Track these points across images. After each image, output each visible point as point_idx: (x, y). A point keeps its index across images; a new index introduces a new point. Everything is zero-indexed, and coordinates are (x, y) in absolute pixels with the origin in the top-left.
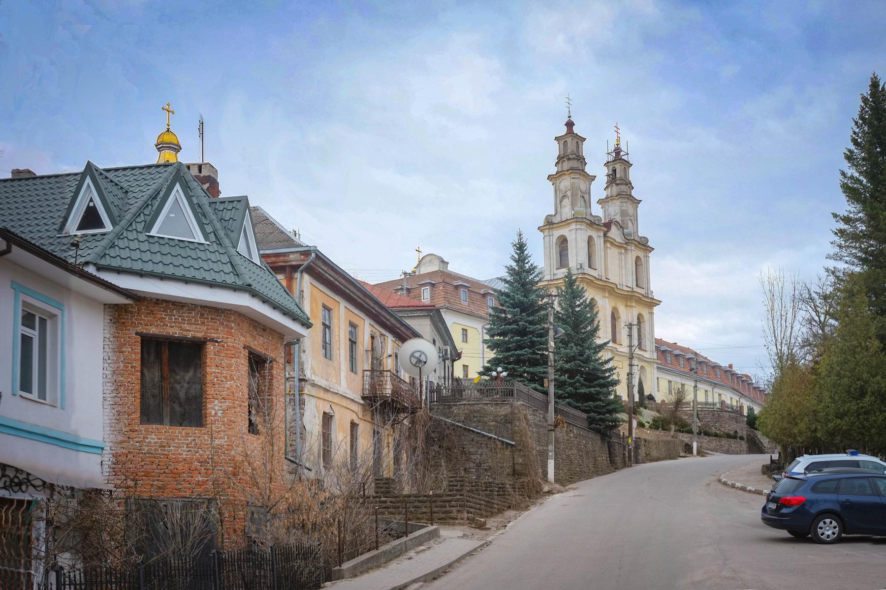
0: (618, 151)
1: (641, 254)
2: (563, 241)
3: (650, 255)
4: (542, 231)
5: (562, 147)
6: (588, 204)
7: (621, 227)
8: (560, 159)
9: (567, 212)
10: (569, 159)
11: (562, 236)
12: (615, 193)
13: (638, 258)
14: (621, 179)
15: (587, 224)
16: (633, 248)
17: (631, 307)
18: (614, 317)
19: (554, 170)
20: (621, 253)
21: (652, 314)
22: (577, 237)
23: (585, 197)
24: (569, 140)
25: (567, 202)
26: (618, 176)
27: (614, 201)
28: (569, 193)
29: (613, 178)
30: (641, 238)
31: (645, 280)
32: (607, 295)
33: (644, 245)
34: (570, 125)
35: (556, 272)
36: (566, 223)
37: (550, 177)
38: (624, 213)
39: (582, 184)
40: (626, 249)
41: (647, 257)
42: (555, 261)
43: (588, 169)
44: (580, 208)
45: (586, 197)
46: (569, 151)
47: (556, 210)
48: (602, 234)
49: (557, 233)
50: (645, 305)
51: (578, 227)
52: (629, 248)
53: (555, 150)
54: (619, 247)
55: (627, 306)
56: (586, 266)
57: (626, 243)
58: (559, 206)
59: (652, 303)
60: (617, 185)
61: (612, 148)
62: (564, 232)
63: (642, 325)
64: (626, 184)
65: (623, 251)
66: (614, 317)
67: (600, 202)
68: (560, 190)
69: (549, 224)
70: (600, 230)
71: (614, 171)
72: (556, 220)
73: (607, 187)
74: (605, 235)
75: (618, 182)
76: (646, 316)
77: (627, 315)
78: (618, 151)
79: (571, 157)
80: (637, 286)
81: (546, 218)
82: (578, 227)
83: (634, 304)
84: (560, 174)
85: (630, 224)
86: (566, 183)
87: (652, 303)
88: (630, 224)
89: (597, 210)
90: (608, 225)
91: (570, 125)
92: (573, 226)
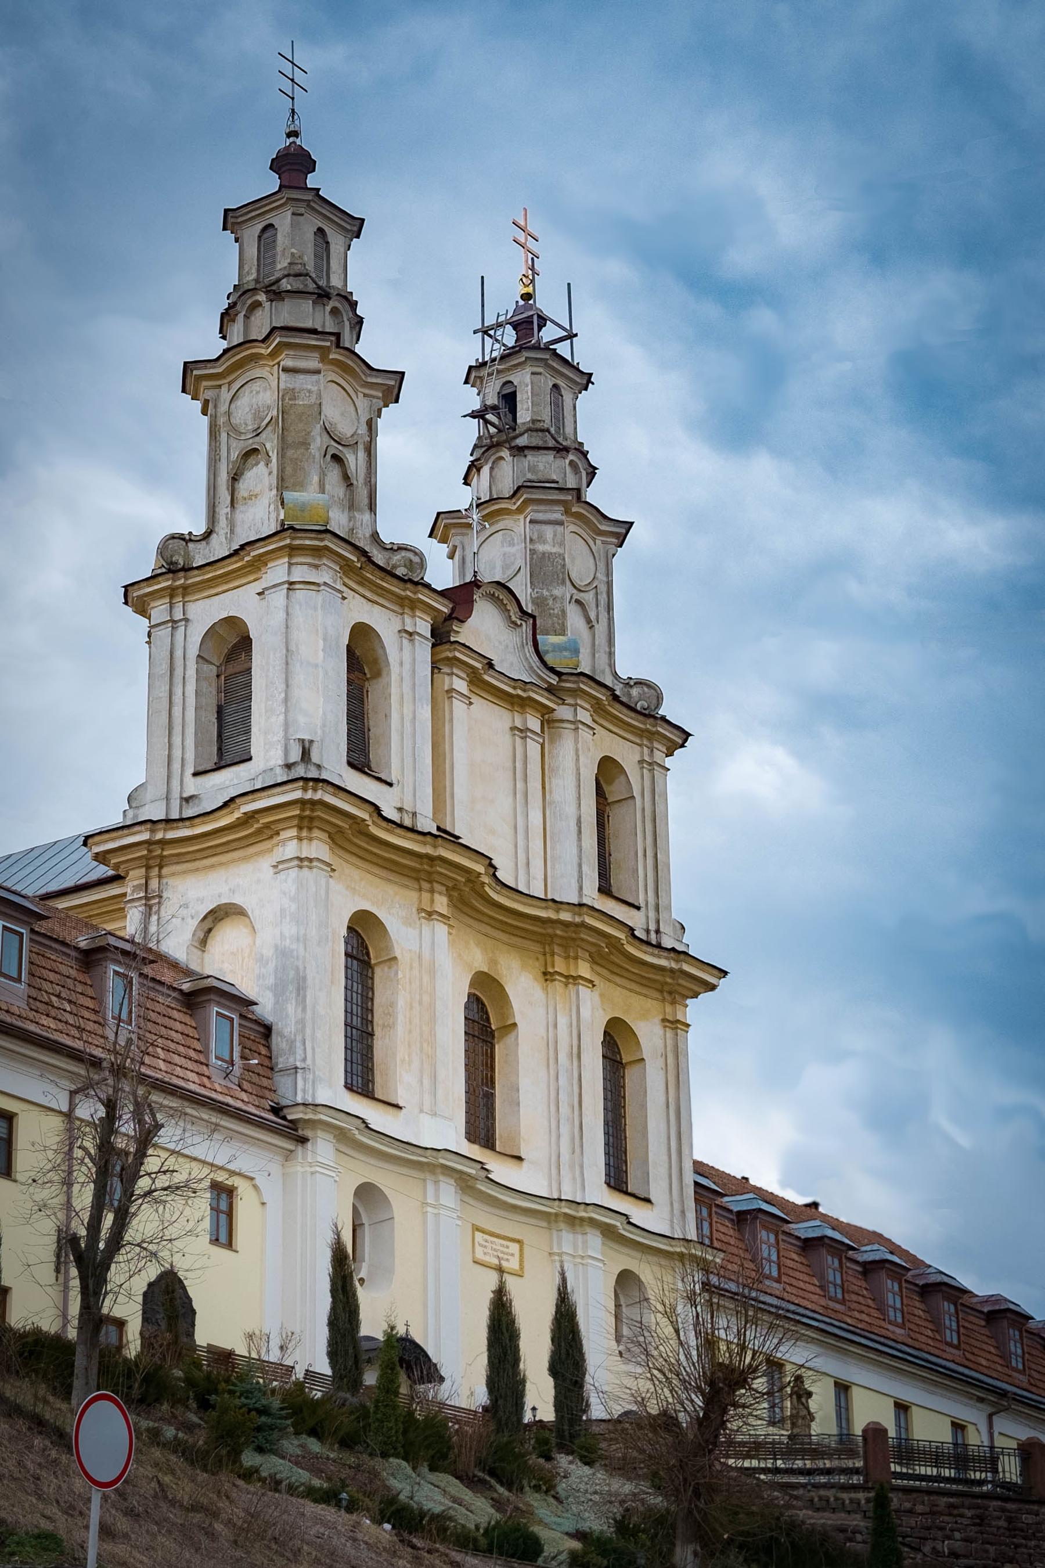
0: (527, 322)
1: (627, 754)
2: (233, 647)
3: (668, 762)
4: (142, 609)
5: (252, 251)
6: (362, 494)
7: (529, 620)
9: (259, 516)
10: (276, 295)
11: (232, 623)
12: (506, 487)
13: (608, 769)
14: (535, 428)
15: (347, 568)
16: (584, 716)
18: (485, 1026)
19: (209, 344)
20: (523, 732)
21: (676, 1026)
22: (299, 629)
23: (351, 463)
24: (283, 221)
25: (260, 478)
26: (524, 416)
27: (505, 522)
29: (501, 429)
30: (629, 684)
31: (644, 869)
32: (441, 903)
33: (643, 717)
34: (293, 164)
36: (247, 559)
37: (193, 376)
38: (544, 568)
39: (340, 411)
40: (549, 721)
41: (652, 767)
43: (375, 348)
44: (318, 495)
45: (355, 461)
46: (282, 264)
48: (423, 626)
49: (206, 612)
50: (645, 983)
51: (300, 573)
52: (563, 712)
55: (548, 976)
56: (334, 763)
57: (550, 690)
59: (678, 978)
60: (519, 451)
61: (504, 302)
62: (240, 602)
63: (631, 1076)
64: (561, 450)
65: (534, 723)
66: (485, 1026)
67: (446, 526)
68: (234, 431)
69: (177, 571)
70: (413, 605)
71: (510, 399)
72: (200, 555)
73: (474, 467)
74: (440, 636)
75: (522, 441)
76: (649, 1034)
77: (553, 1025)
78: (527, 322)
79: (286, 285)
80: (605, 890)
81: (163, 550)
82: (300, 573)
83: (584, 969)
84: (237, 359)
85: (575, 620)
86: (258, 395)
87: (678, 978)
88: (575, 620)
89: (402, 519)
90: (461, 598)
91: (293, 164)
92: (277, 571)
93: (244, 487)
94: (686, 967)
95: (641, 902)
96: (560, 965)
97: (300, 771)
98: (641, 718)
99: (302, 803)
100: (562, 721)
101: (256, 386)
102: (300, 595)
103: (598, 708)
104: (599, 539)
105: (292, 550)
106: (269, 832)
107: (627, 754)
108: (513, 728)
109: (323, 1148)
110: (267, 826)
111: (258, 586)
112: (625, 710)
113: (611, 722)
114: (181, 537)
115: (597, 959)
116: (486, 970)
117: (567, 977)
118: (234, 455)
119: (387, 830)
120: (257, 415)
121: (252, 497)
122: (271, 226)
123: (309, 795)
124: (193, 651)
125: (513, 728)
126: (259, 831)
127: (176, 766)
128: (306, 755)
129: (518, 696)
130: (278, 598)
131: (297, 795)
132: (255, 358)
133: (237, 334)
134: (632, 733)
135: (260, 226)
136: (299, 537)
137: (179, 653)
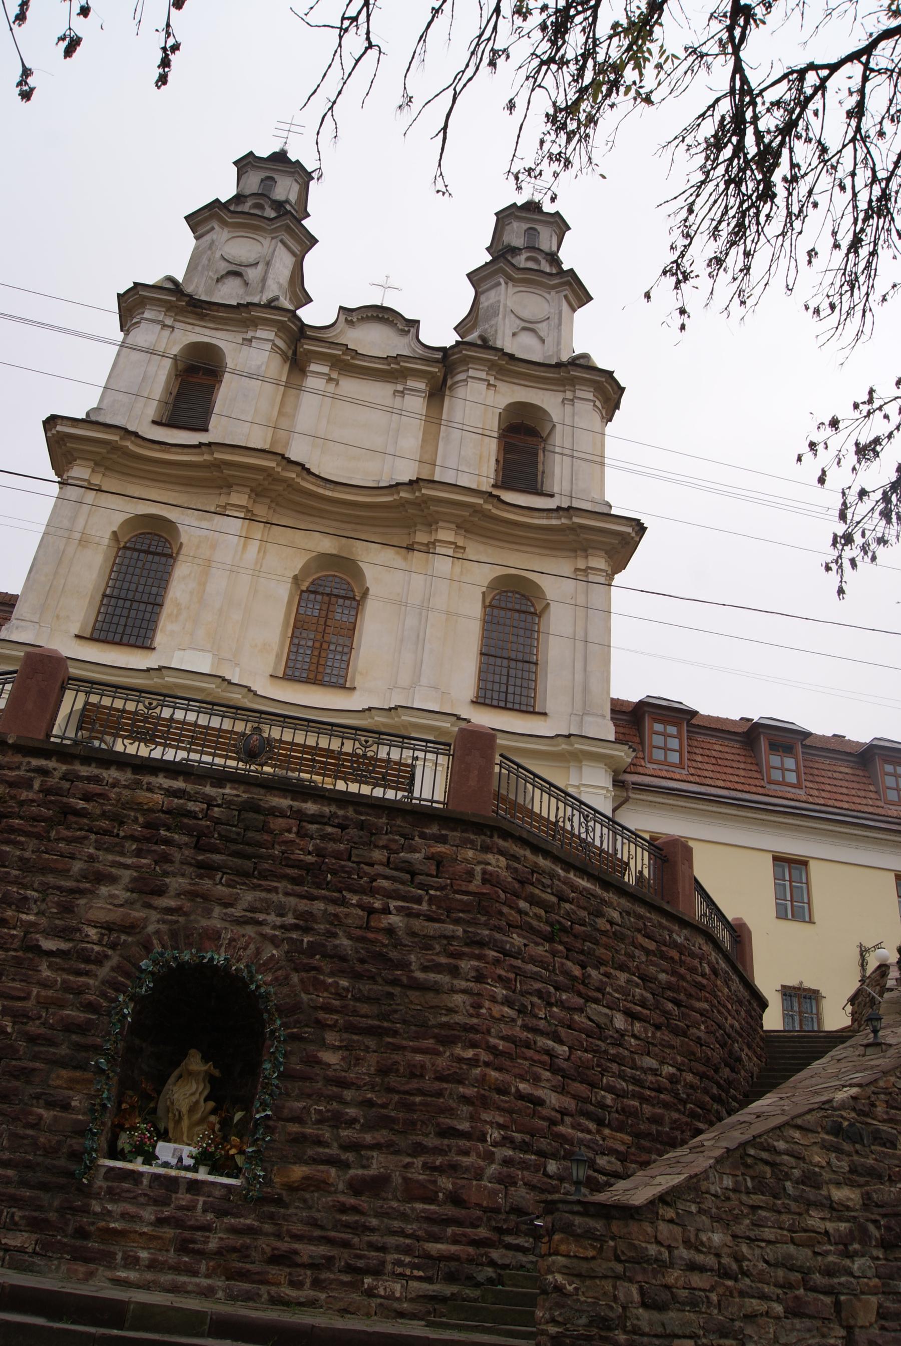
54: (392, 371)
65: (421, 385)
83: (446, 535)
94: (576, 520)
95: (556, 489)
96: (421, 537)
98: (552, 370)
100: (457, 382)
103: (492, 366)
104: (553, 293)
107: (548, 400)
108: (395, 391)
112: (537, 368)
113: (526, 380)
115: (463, 527)
116: (334, 552)
117: (427, 545)
119: (163, 451)
125: (395, 391)
129: (396, 370)
134: (555, 384)
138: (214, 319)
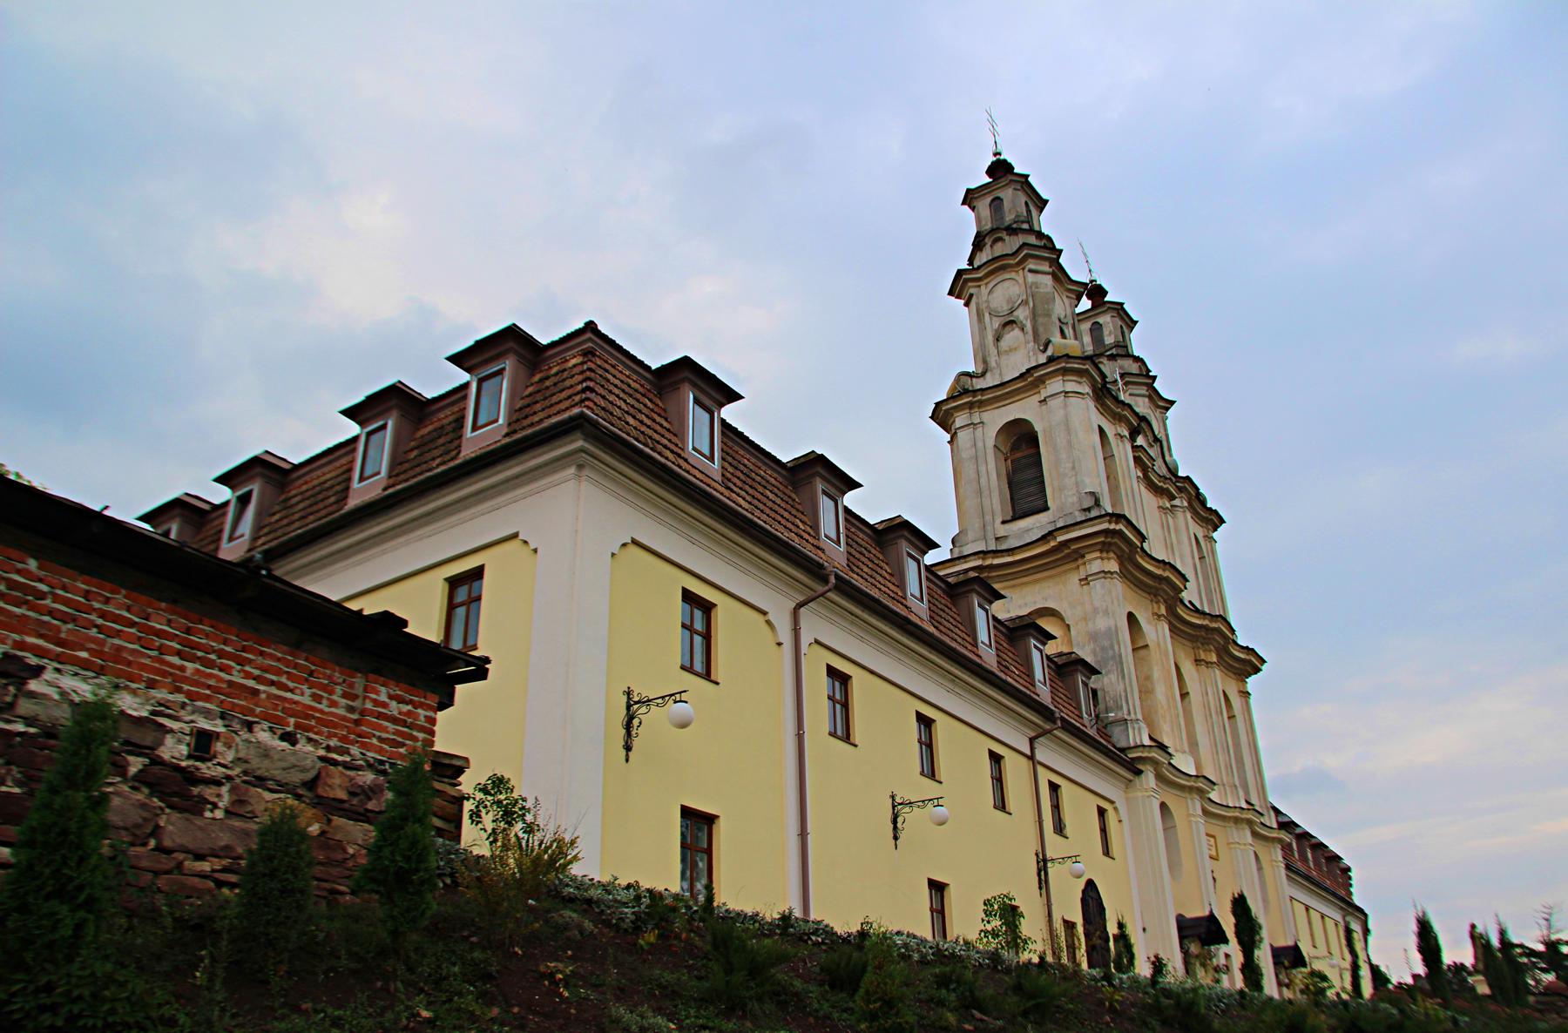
2: (1021, 439)
8: (978, 244)
17: (1208, 664)
28: (1022, 314)
34: (1000, 169)
35: (1002, 530)
36: (1030, 380)
42: (996, 498)
47: (985, 362)
51: (1070, 387)
53: (967, 224)
55: (1197, 661)
58: (993, 351)
62: (1024, 409)
82: (1070, 387)
86: (1004, 292)
92: (1055, 385)
93: (1004, 344)
97: (1094, 513)
99: (1106, 532)
101: (1006, 284)
102: (1073, 400)
105: (1065, 372)
106: (1078, 556)
109: (1149, 778)
110: (1076, 551)
111: (1037, 398)
114: (967, 374)
118: (996, 325)
120: (1009, 301)
121: (1012, 350)
122: (998, 198)
123: (1112, 526)
124: (991, 442)
126: (1068, 555)
127: (988, 518)
128: (1097, 503)
130: (1053, 403)
131: (1105, 526)
132: (1003, 268)
133: (982, 258)
135: (989, 199)
136: (1061, 364)
137: (980, 444)
138: (1103, 405)
